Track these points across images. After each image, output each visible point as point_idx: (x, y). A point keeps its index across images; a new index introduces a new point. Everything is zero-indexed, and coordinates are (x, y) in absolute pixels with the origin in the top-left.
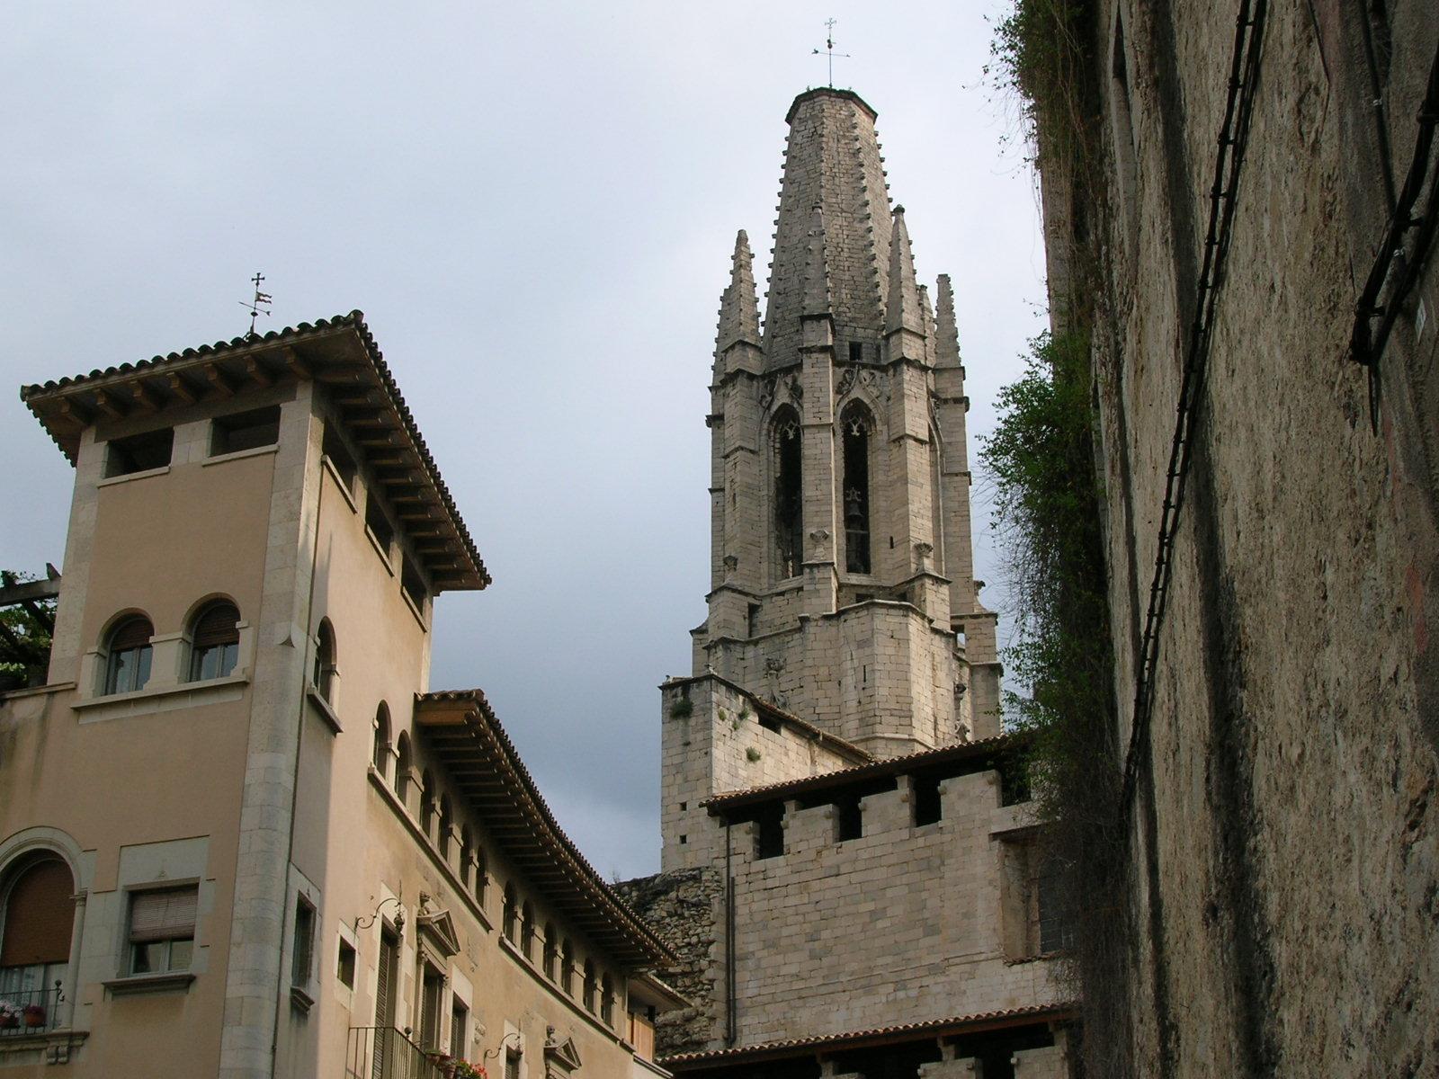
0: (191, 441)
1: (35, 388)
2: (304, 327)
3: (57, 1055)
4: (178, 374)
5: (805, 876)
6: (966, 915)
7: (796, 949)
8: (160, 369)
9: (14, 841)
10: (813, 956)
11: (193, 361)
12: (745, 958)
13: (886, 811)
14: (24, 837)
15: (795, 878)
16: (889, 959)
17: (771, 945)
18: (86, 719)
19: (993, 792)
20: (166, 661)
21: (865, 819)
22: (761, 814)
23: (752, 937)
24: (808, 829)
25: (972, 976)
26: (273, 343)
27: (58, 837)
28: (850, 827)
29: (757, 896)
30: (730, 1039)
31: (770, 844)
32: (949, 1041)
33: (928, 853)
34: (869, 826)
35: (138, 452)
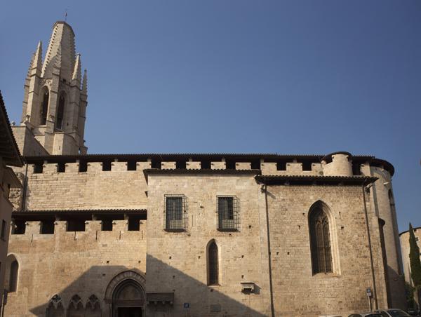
6: (91, 194)
7: (43, 196)
10: (48, 198)
13: (73, 167)
17: (35, 194)
21: (66, 168)
28: (61, 169)
31: (39, 170)
34: (67, 169)
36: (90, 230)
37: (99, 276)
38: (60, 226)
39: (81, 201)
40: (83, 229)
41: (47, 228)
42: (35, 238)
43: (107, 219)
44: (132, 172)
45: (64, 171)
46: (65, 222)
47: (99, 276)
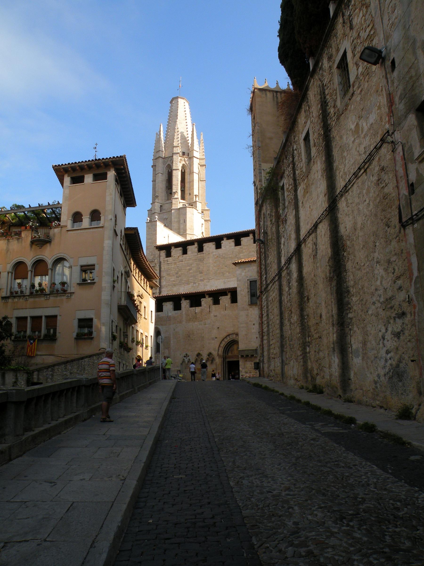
0: (89, 178)
1: (56, 166)
2: (114, 157)
3: (68, 296)
4: (87, 165)
5: (176, 261)
6: (208, 270)
8: (83, 164)
9: (55, 256)
10: (177, 277)
11: (90, 162)
12: (163, 277)
13: (192, 249)
14: (58, 255)
15: (174, 262)
16: (192, 278)
17: (169, 275)
18: (69, 232)
19: (214, 247)
20: (86, 222)
22: (167, 249)
23: (164, 273)
24: (176, 252)
25: (209, 282)
26: (107, 160)
27: (65, 255)
28: (185, 252)
29: (166, 265)
30: (160, 293)
31: (169, 255)
32: (207, 294)
33: (200, 258)
34: (189, 252)
35: (77, 180)
36: (205, 305)
37: (213, 339)
38: (185, 304)
39: (201, 277)
40: (199, 305)
41: (177, 307)
42: (170, 314)
43: (216, 296)
44: (238, 247)
45: (187, 254)
46: (188, 301)
47: (213, 339)
